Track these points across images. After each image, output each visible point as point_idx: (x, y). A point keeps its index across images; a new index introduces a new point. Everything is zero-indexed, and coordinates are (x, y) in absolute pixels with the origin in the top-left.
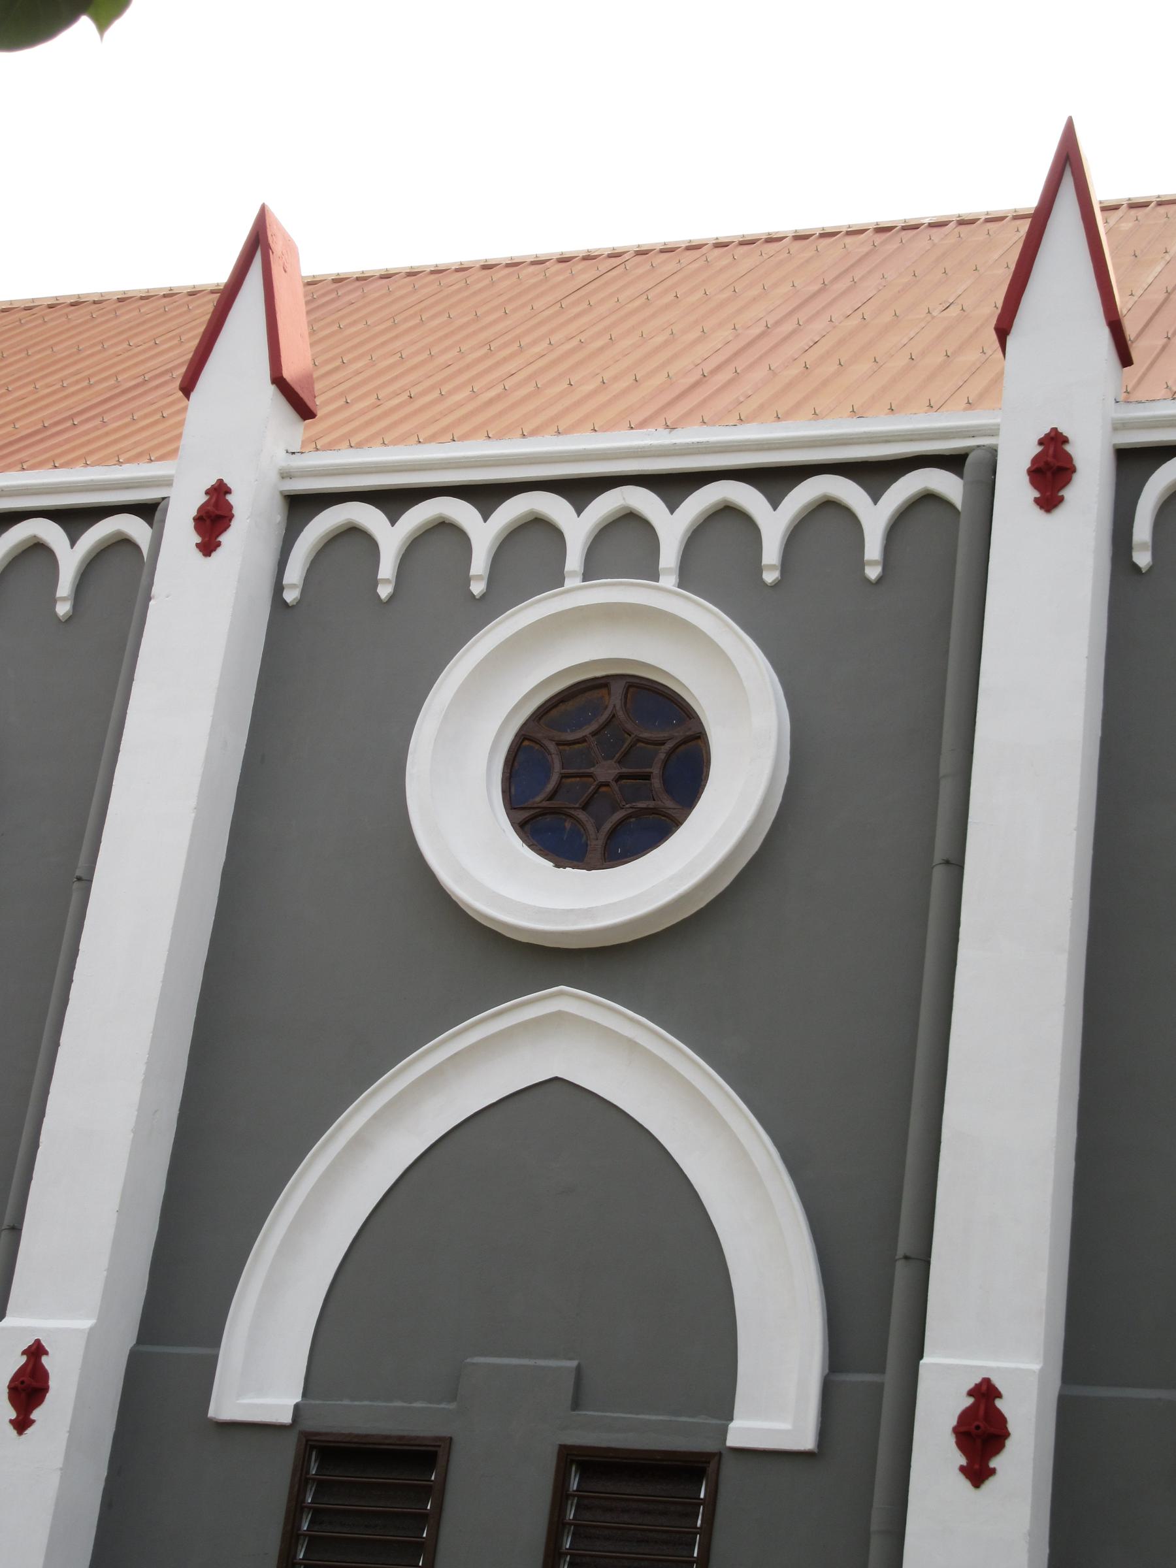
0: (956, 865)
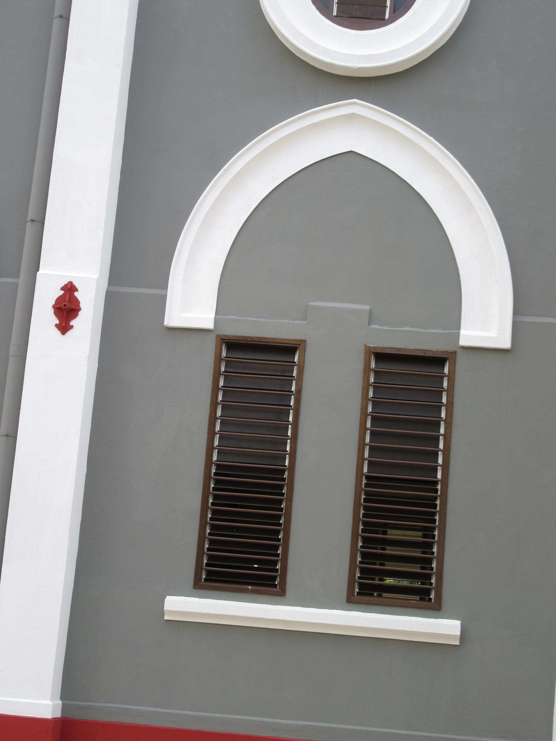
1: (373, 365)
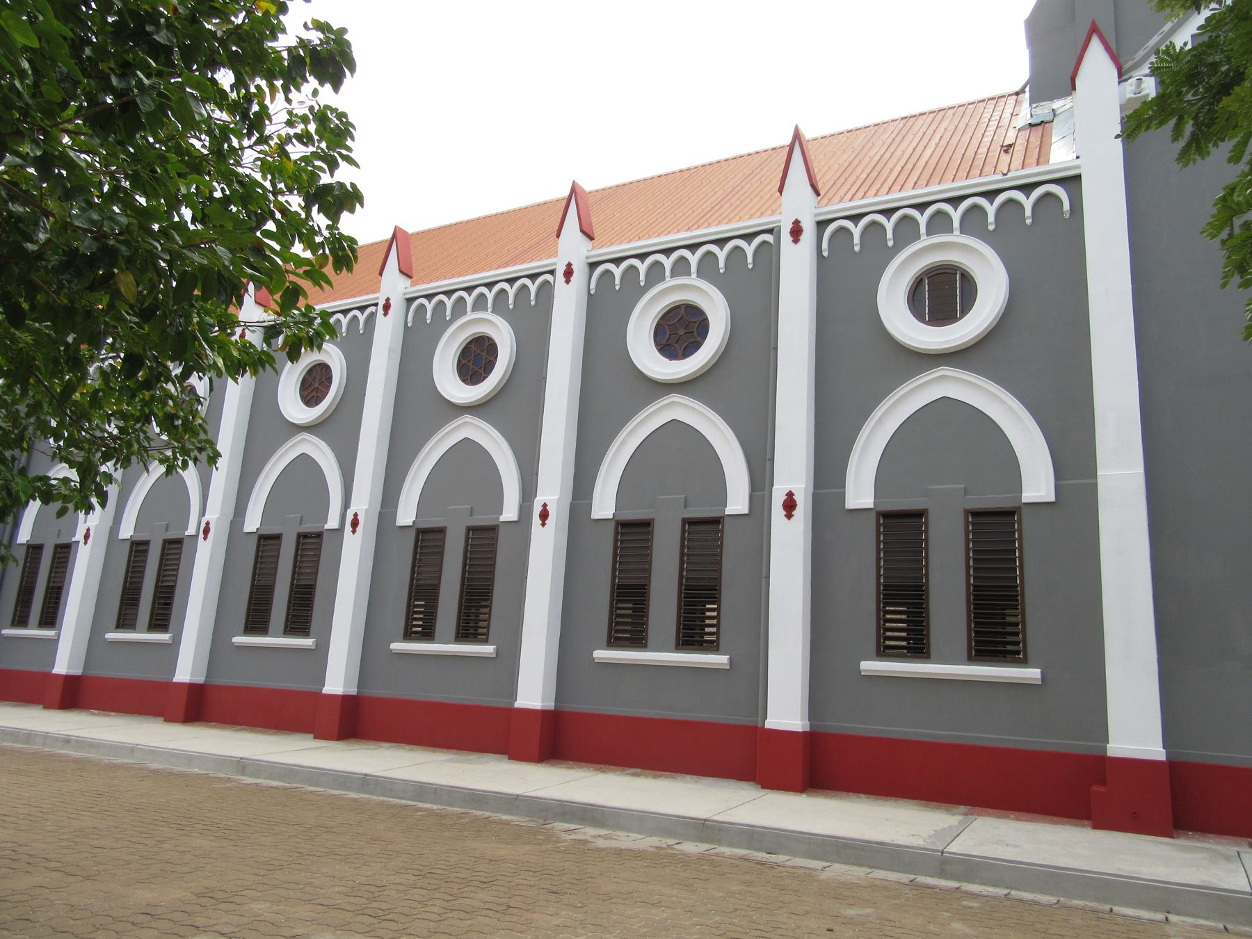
1: (970, 520)
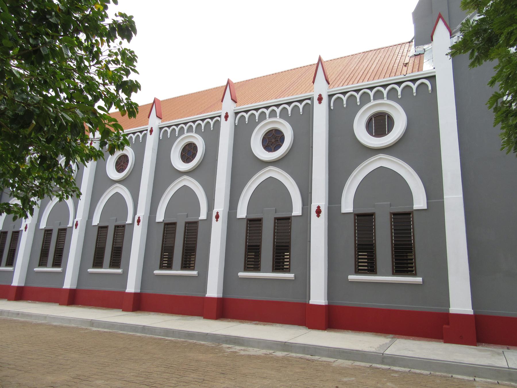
0: (312, 147)
1: (393, 217)
